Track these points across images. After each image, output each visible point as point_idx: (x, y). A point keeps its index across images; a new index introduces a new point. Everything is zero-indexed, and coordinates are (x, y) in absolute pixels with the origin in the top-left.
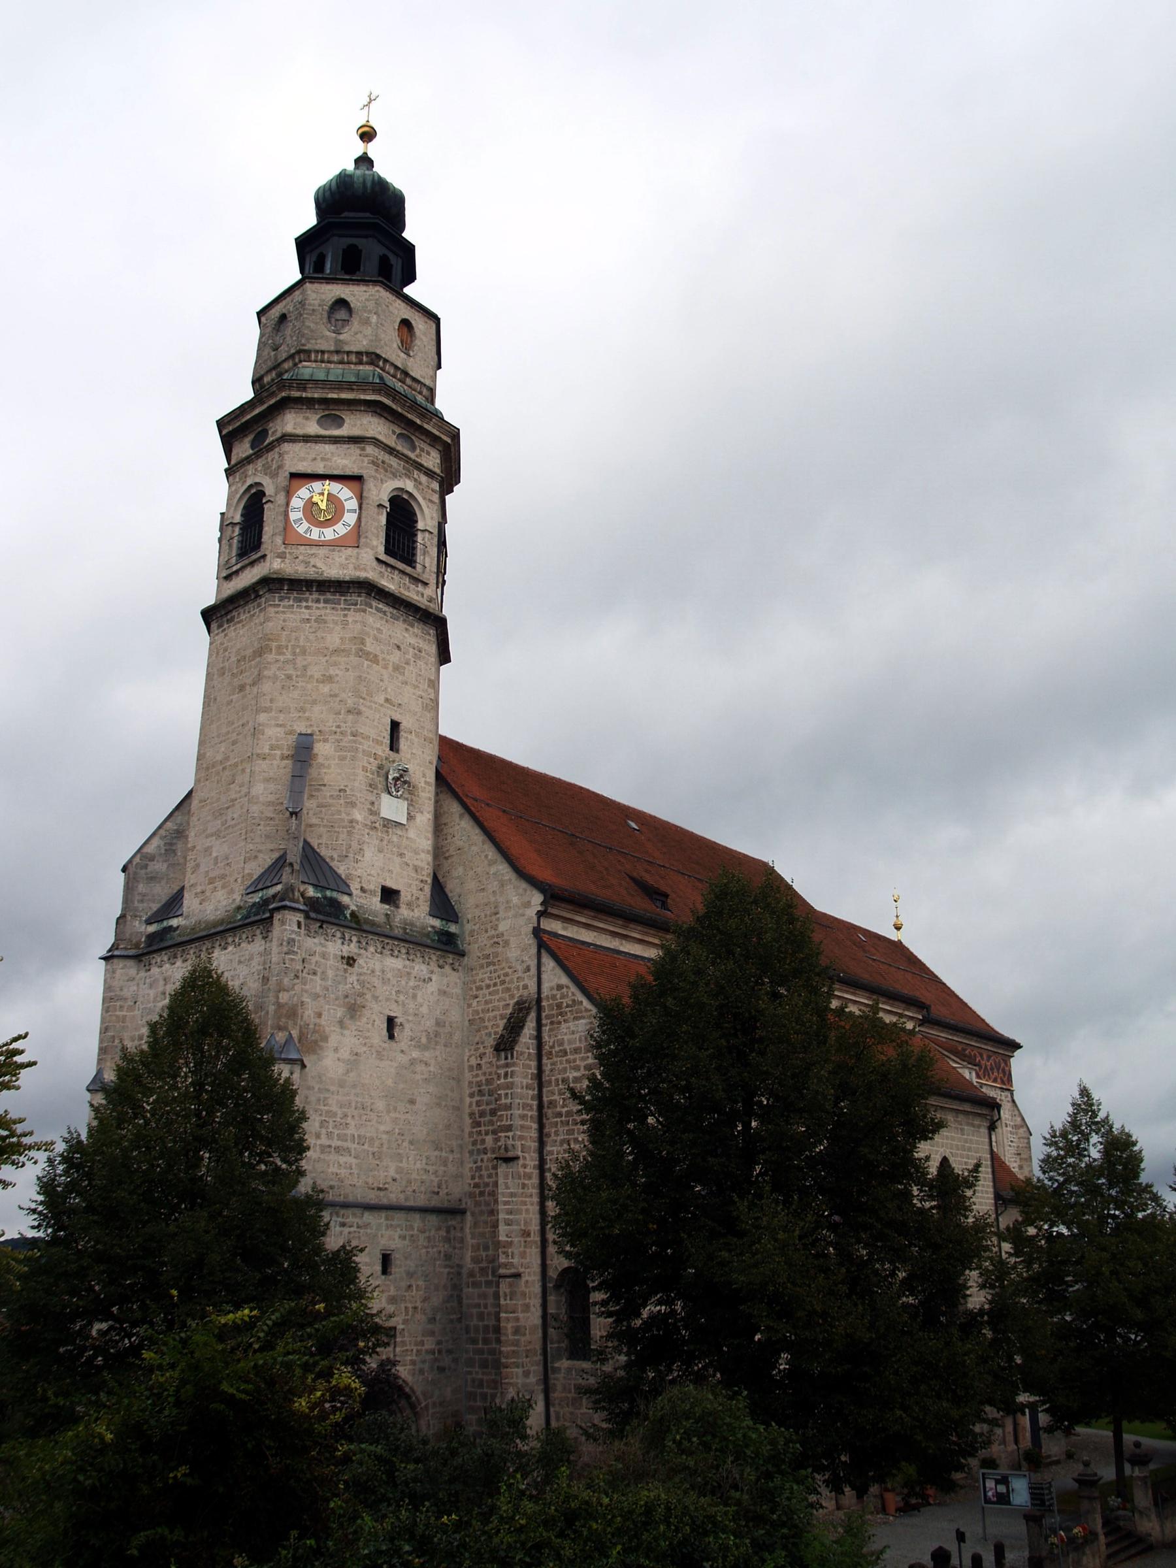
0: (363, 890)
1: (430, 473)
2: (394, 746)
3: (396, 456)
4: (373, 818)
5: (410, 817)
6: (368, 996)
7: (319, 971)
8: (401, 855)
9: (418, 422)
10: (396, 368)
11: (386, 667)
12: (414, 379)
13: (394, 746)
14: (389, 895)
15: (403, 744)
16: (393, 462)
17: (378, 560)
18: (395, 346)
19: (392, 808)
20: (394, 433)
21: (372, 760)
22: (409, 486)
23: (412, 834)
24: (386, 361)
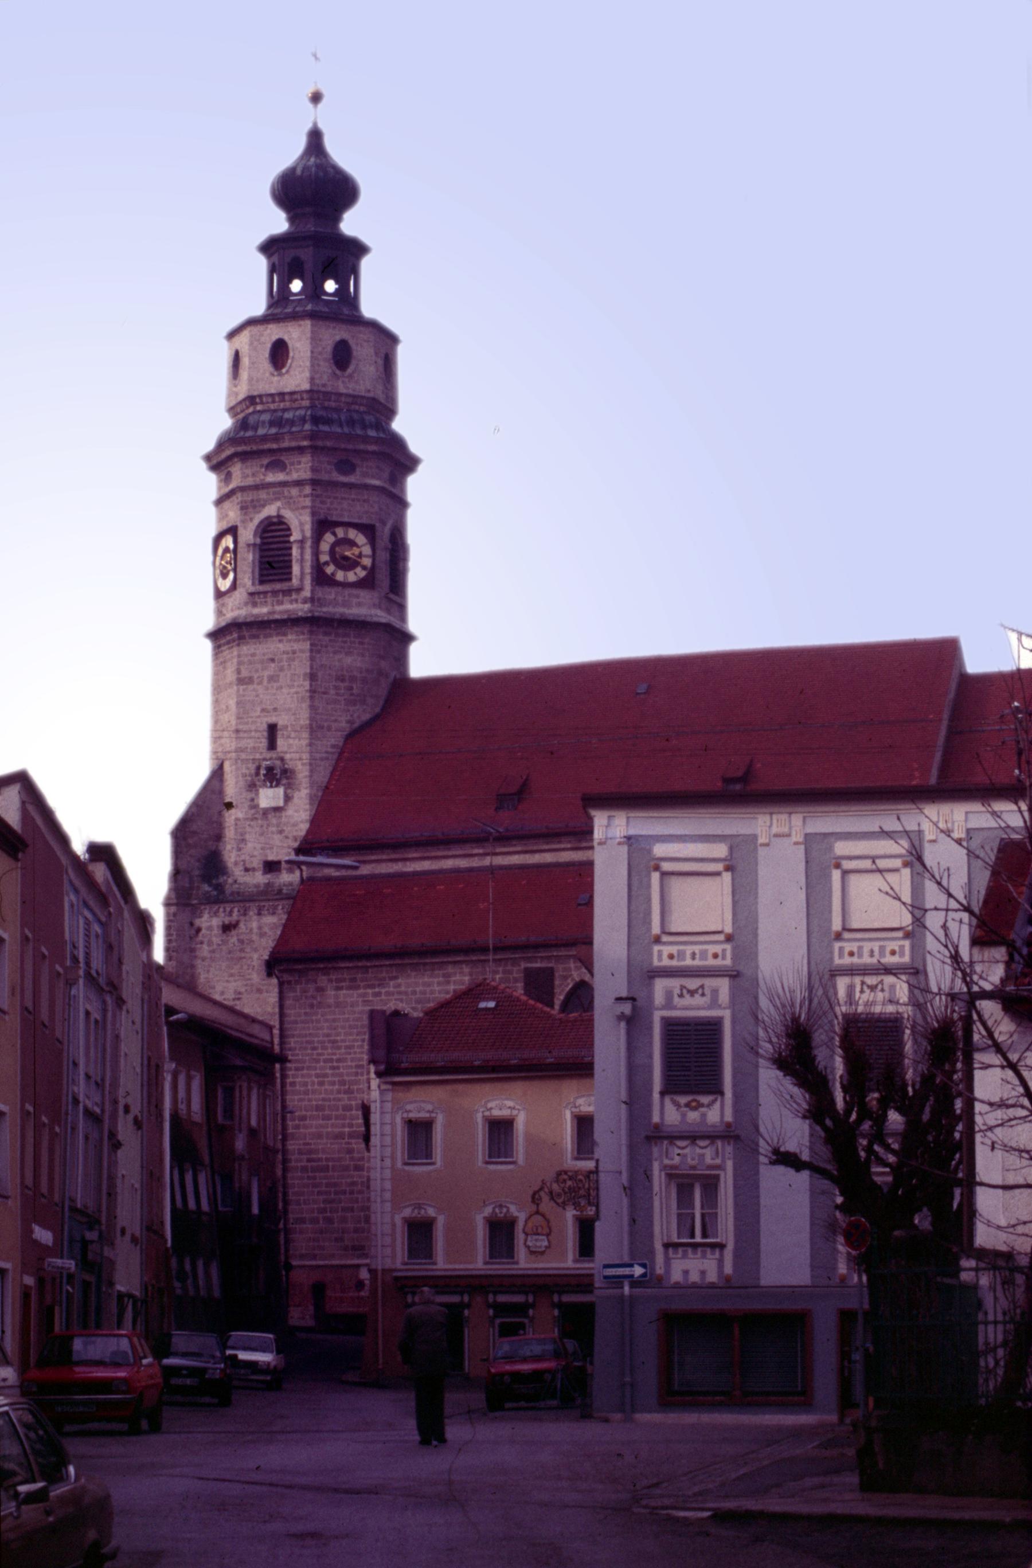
0: (247, 870)
1: (299, 483)
2: (272, 745)
3: (263, 488)
4: (253, 811)
5: (287, 798)
6: (248, 950)
7: (206, 940)
8: (281, 832)
9: (275, 446)
10: (272, 395)
11: (260, 683)
12: (292, 393)
13: (272, 745)
14: (271, 867)
15: (280, 742)
16: (263, 495)
17: (251, 594)
18: (267, 375)
19: (269, 797)
20: (262, 466)
21: (250, 765)
22: (270, 510)
23: (290, 812)
24: (260, 396)
